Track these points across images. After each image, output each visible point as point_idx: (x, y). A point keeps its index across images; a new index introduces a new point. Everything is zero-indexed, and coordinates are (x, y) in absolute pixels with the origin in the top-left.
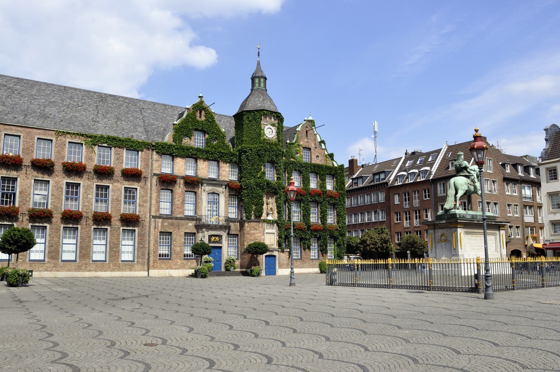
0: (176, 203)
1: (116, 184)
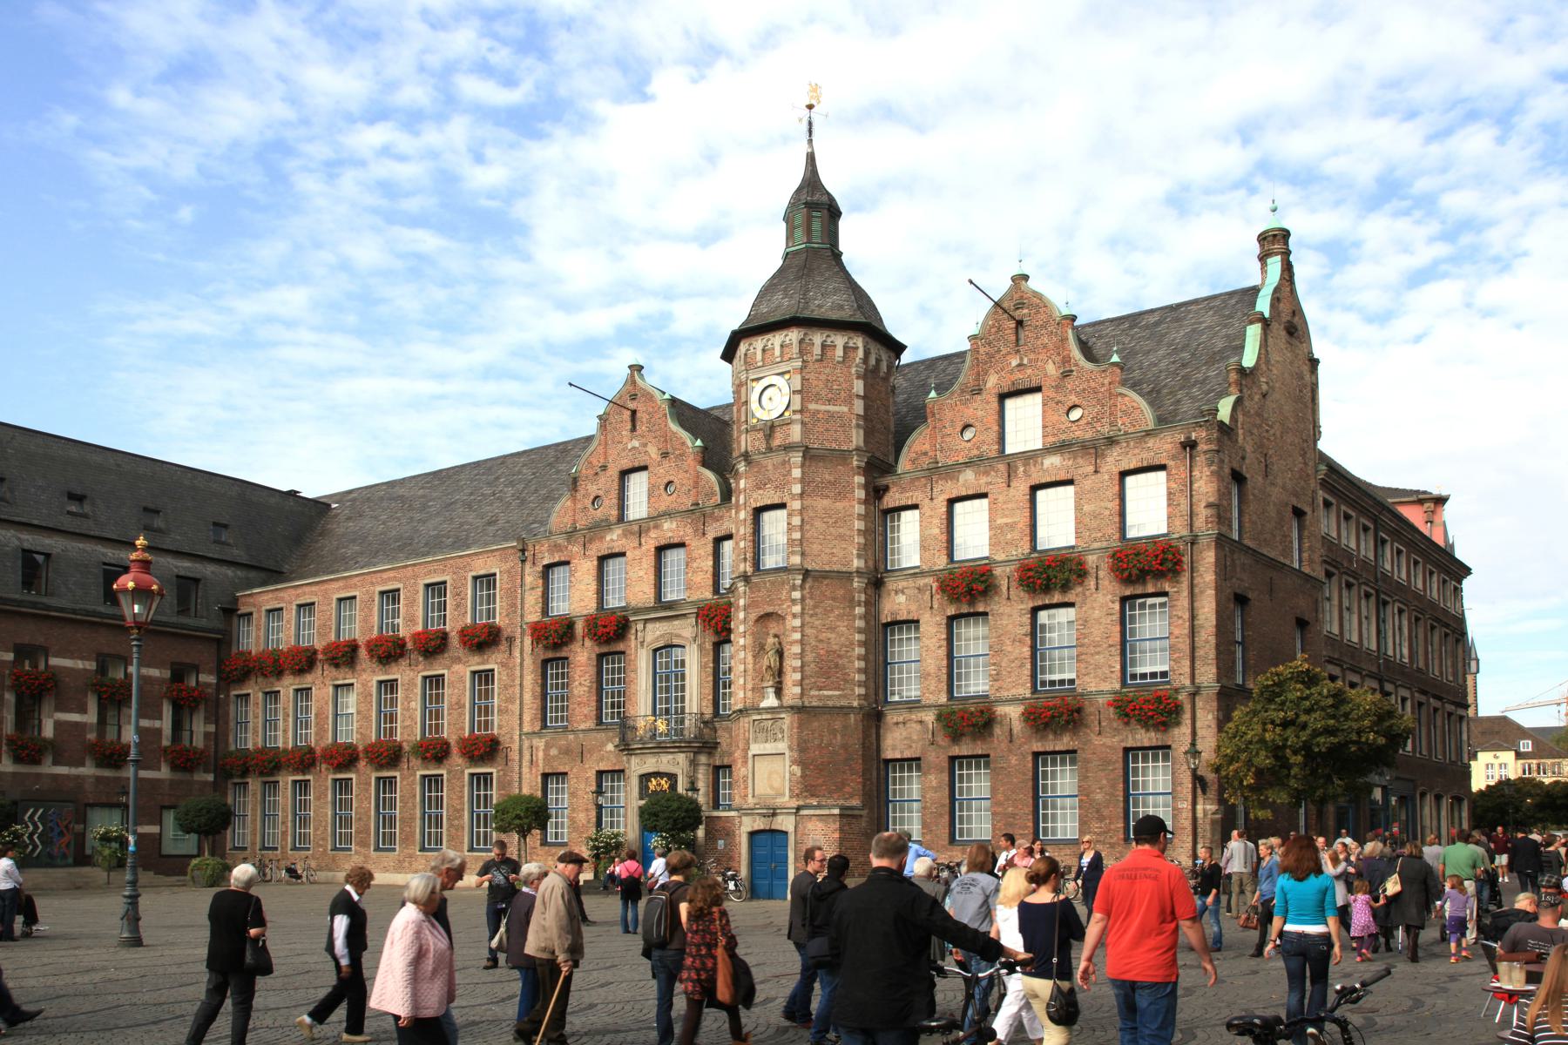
1: (457, 667)
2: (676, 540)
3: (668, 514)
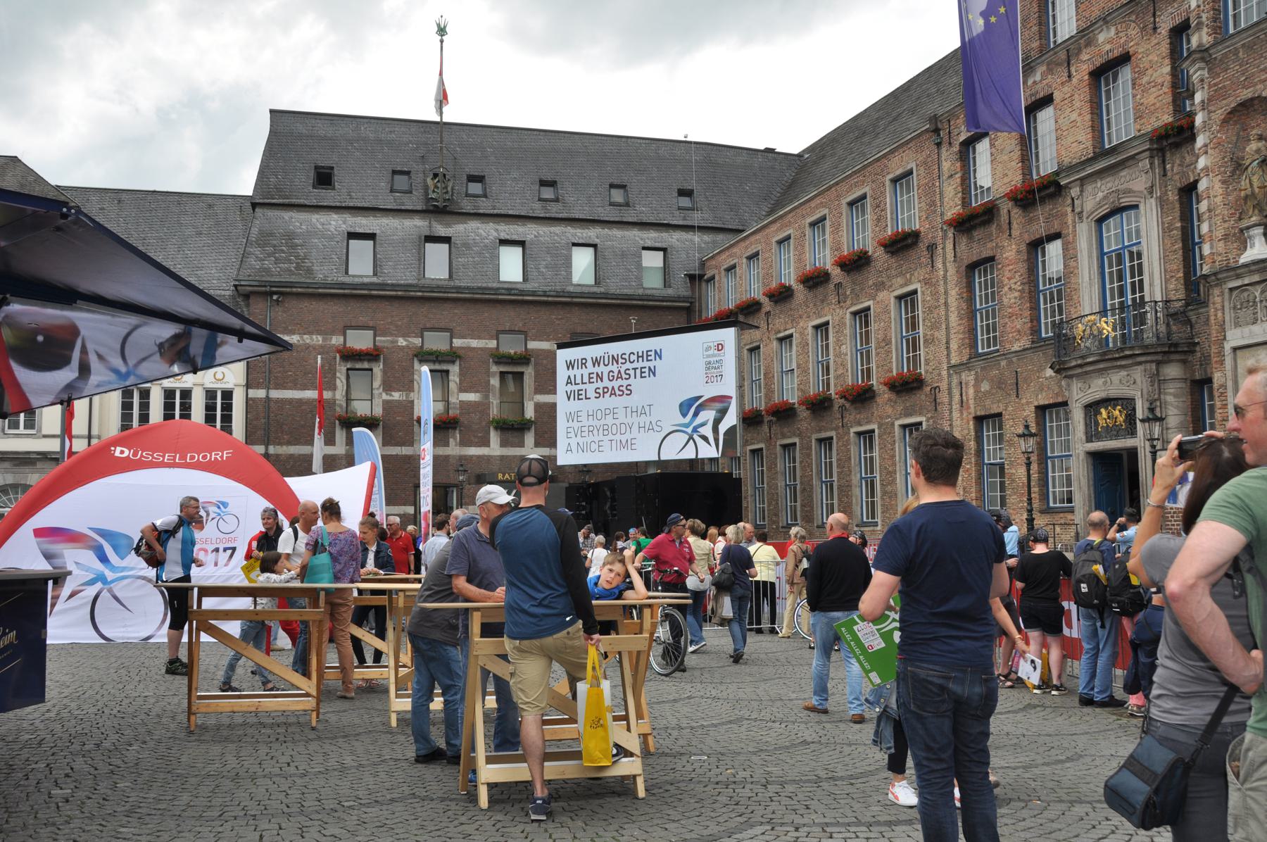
0: (1005, 301)
1: (882, 295)
2: (1116, 53)
3: (1105, 20)
